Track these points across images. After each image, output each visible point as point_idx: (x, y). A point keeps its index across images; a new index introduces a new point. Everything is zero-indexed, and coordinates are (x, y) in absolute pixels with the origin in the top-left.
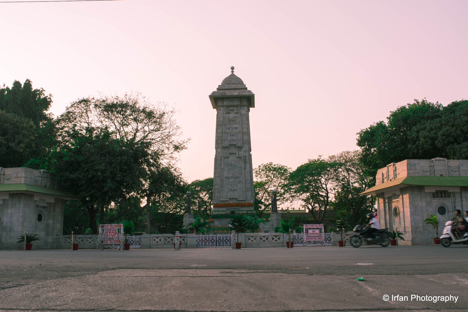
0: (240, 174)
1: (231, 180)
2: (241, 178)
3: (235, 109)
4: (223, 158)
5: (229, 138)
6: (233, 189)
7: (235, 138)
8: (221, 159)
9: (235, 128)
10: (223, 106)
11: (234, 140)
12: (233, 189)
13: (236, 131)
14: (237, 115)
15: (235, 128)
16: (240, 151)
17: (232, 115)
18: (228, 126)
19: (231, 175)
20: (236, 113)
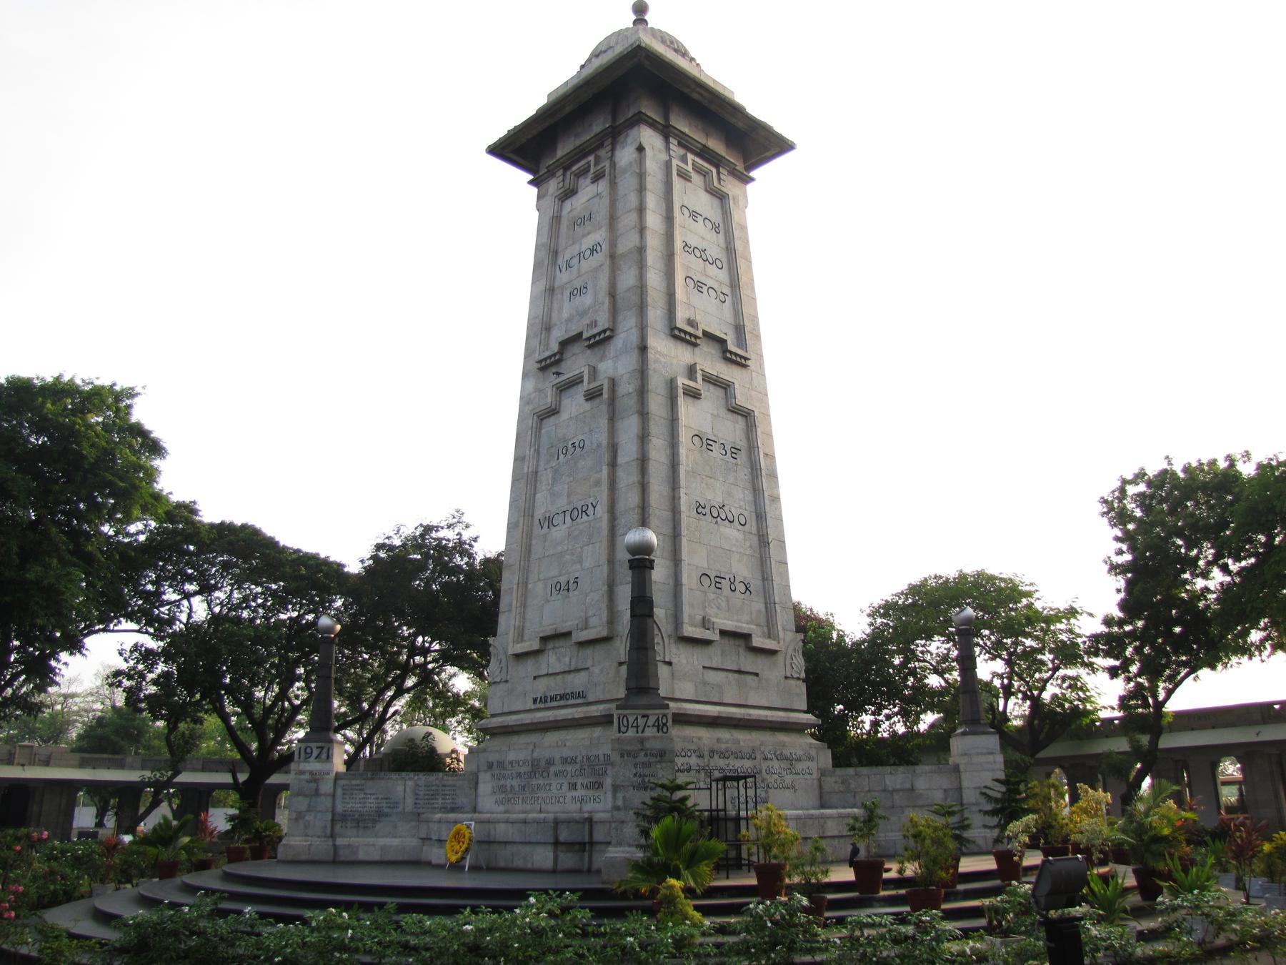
3: (591, 158)
6: (563, 579)
19: (562, 503)
20: (597, 178)
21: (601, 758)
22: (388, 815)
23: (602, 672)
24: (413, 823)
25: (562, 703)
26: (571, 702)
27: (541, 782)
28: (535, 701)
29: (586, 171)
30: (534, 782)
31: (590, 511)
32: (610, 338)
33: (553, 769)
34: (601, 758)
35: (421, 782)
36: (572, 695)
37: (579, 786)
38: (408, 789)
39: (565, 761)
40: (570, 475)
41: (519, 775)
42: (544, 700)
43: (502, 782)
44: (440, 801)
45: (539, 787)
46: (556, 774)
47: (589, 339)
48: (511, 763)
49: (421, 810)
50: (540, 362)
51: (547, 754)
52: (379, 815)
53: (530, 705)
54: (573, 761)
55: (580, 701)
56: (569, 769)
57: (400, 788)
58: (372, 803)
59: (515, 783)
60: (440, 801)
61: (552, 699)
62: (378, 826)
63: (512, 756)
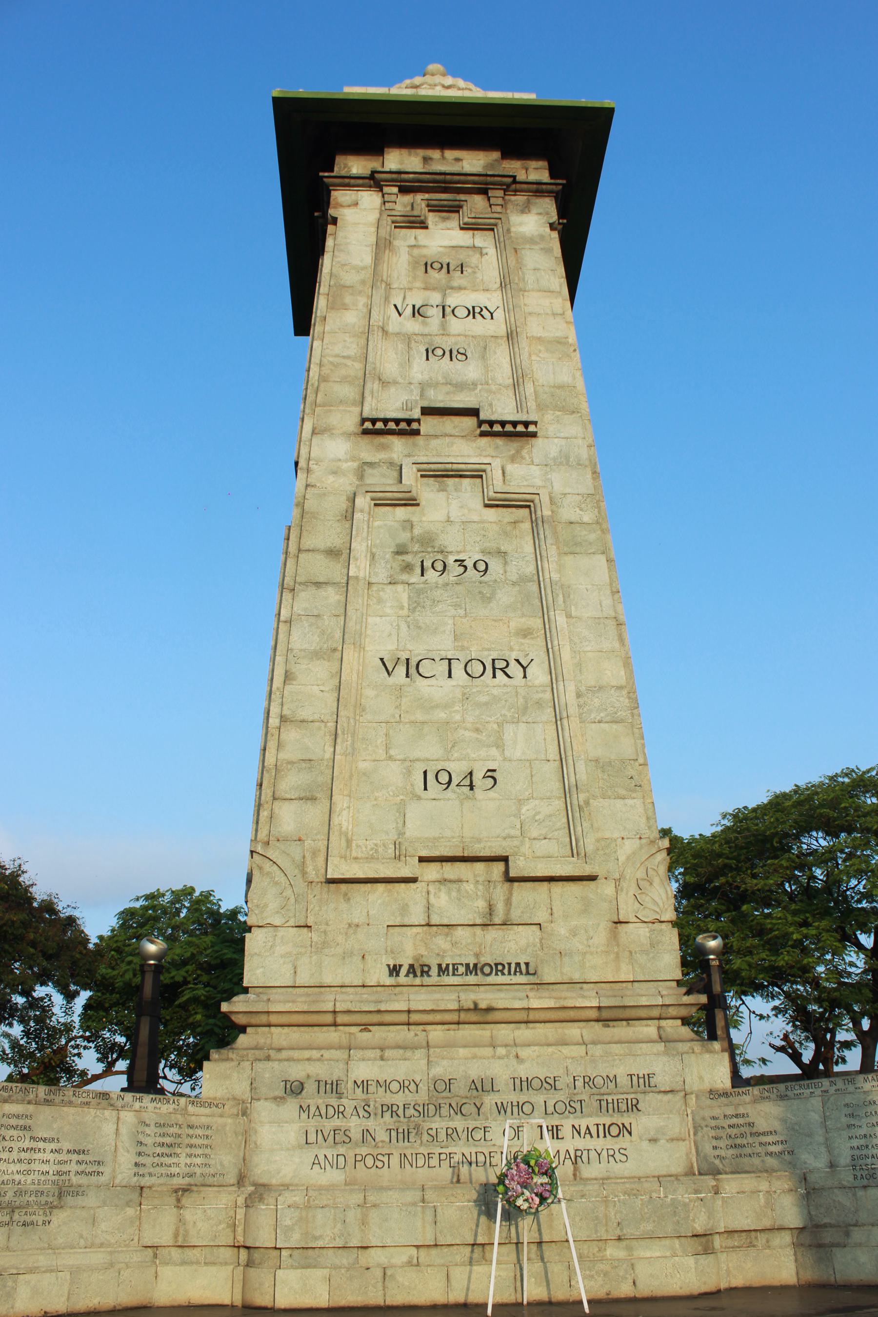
0: (526, 633)
1: (436, 687)
2: (538, 674)
4: (362, 502)
5: (420, 370)
6: (458, 769)
7: (471, 371)
8: (349, 515)
9: (472, 312)
10: (374, 181)
11: (461, 386)
12: (458, 769)
13: (479, 326)
14: (482, 240)
15: (472, 312)
16: (513, 459)
17: (443, 236)
18: (416, 298)
19: (444, 645)
21: (623, 1081)
22: (78, 1191)
23: (574, 933)
24: (130, 1212)
25: (471, 979)
26: (492, 979)
27: (459, 1123)
28: (394, 970)
29: (455, 209)
30: (438, 1124)
31: (515, 670)
32: (534, 435)
33: (489, 1101)
34: (623, 1081)
35: (147, 1117)
36: (498, 968)
37: (566, 1132)
38: (123, 1130)
39: (523, 1084)
40: (457, 606)
41: (391, 1109)
42: (419, 970)
43: (337, 1122)
44: (183, 1160)
45: (453, 1133)
46: (501, 1109)
47: (491, 423)
48: (364, 1085)
49: (146, 1181)
50: (374, 421)
51: (475, 1071)
52: (63, 1193)
53: (379, 975)
54: (551, 1084)
55: (522, 979)
56: (539, 1099)
57: (109, 1128)
58: (45, 1164)
59: (379, 1126)
60: (183, 1160)
61: (442, 970)
62: (59, 1217)
63: (364, 1069)
